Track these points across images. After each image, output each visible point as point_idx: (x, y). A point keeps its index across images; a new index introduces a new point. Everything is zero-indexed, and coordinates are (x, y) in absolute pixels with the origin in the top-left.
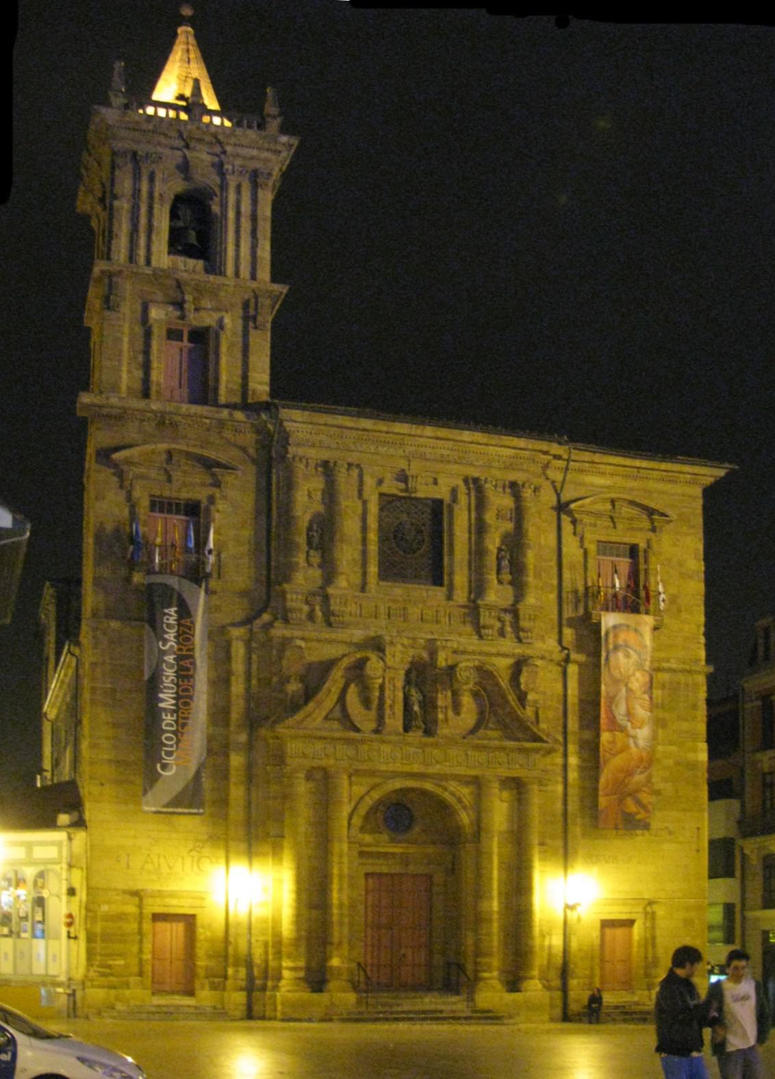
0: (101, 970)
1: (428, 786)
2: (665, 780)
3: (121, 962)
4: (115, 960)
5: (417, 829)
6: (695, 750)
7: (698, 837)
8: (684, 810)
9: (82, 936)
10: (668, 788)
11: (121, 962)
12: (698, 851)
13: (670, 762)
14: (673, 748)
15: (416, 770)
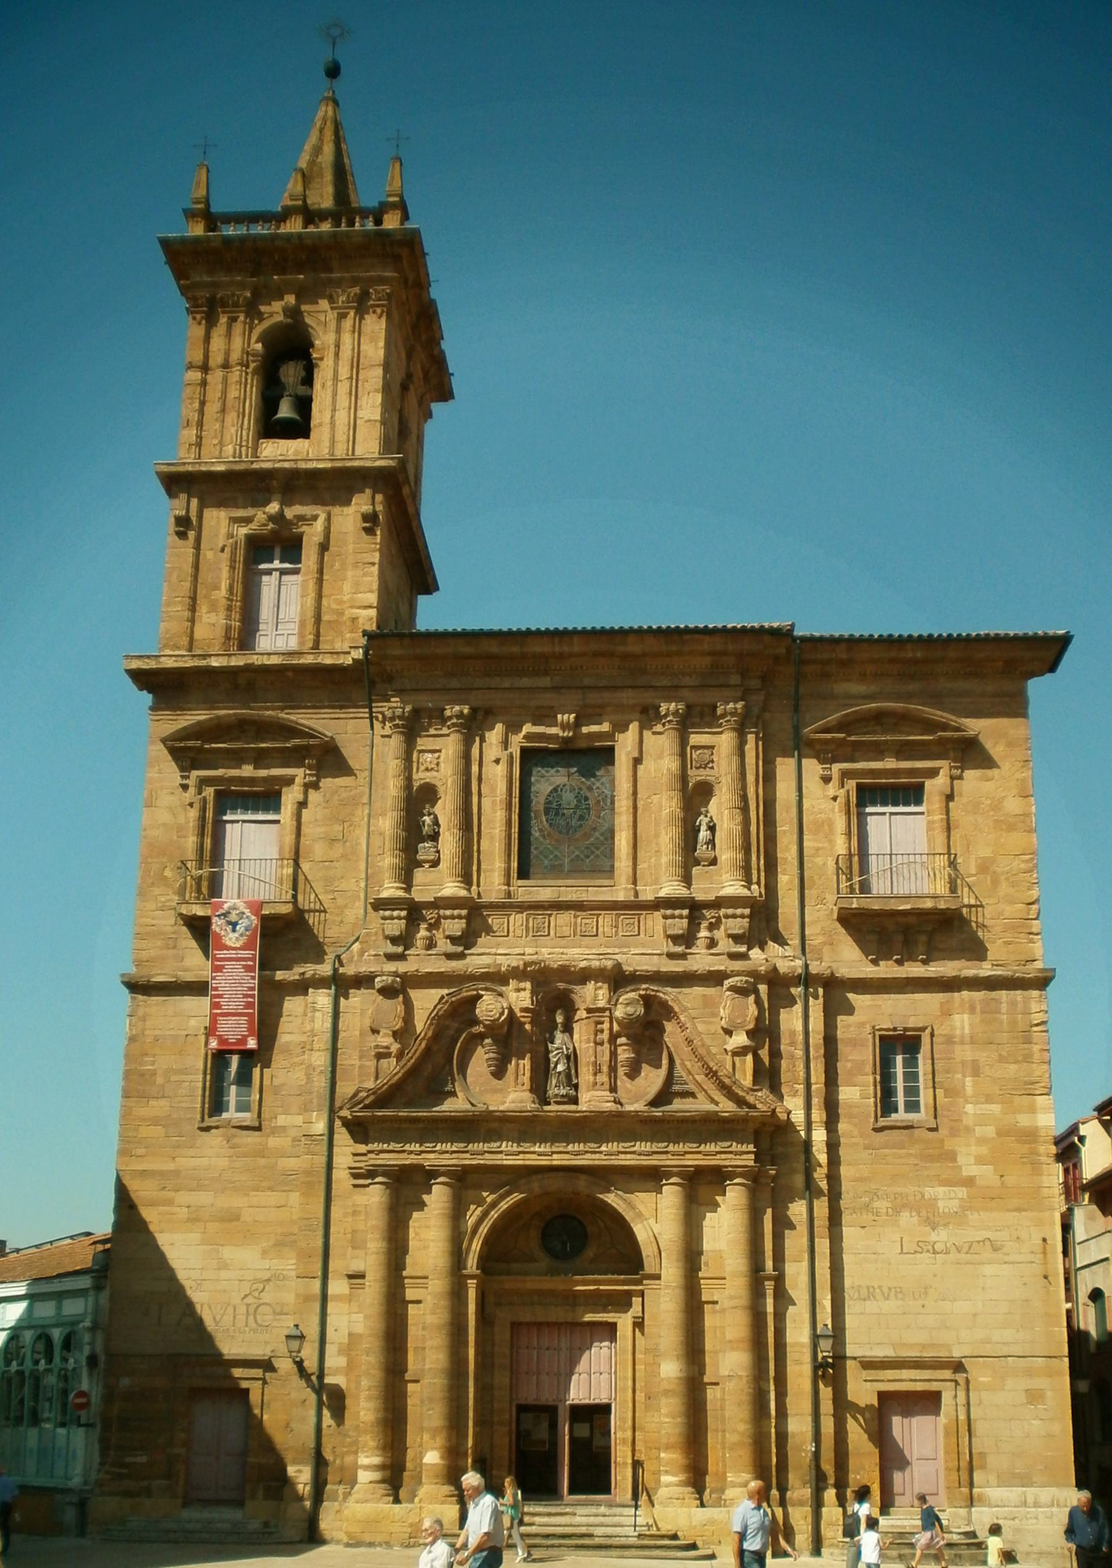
0: (113, 1469)
1: (582, 1184)
2: (980, 1160)
3: (143, 1459)
4: (136, 1456)
5: (590, 1252)
6: (1032, 1110)
7: (1044, 1253)
8: (1019, 1210)
9: (99, 1426)
10: (985, 1174)
11: (143, 1459)
12: (1046, 1277)
13: (990, 1131)
14: (996, 1108)
15: (555, 1163)
